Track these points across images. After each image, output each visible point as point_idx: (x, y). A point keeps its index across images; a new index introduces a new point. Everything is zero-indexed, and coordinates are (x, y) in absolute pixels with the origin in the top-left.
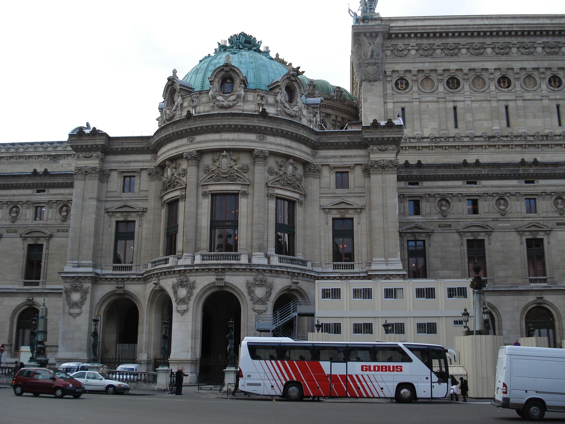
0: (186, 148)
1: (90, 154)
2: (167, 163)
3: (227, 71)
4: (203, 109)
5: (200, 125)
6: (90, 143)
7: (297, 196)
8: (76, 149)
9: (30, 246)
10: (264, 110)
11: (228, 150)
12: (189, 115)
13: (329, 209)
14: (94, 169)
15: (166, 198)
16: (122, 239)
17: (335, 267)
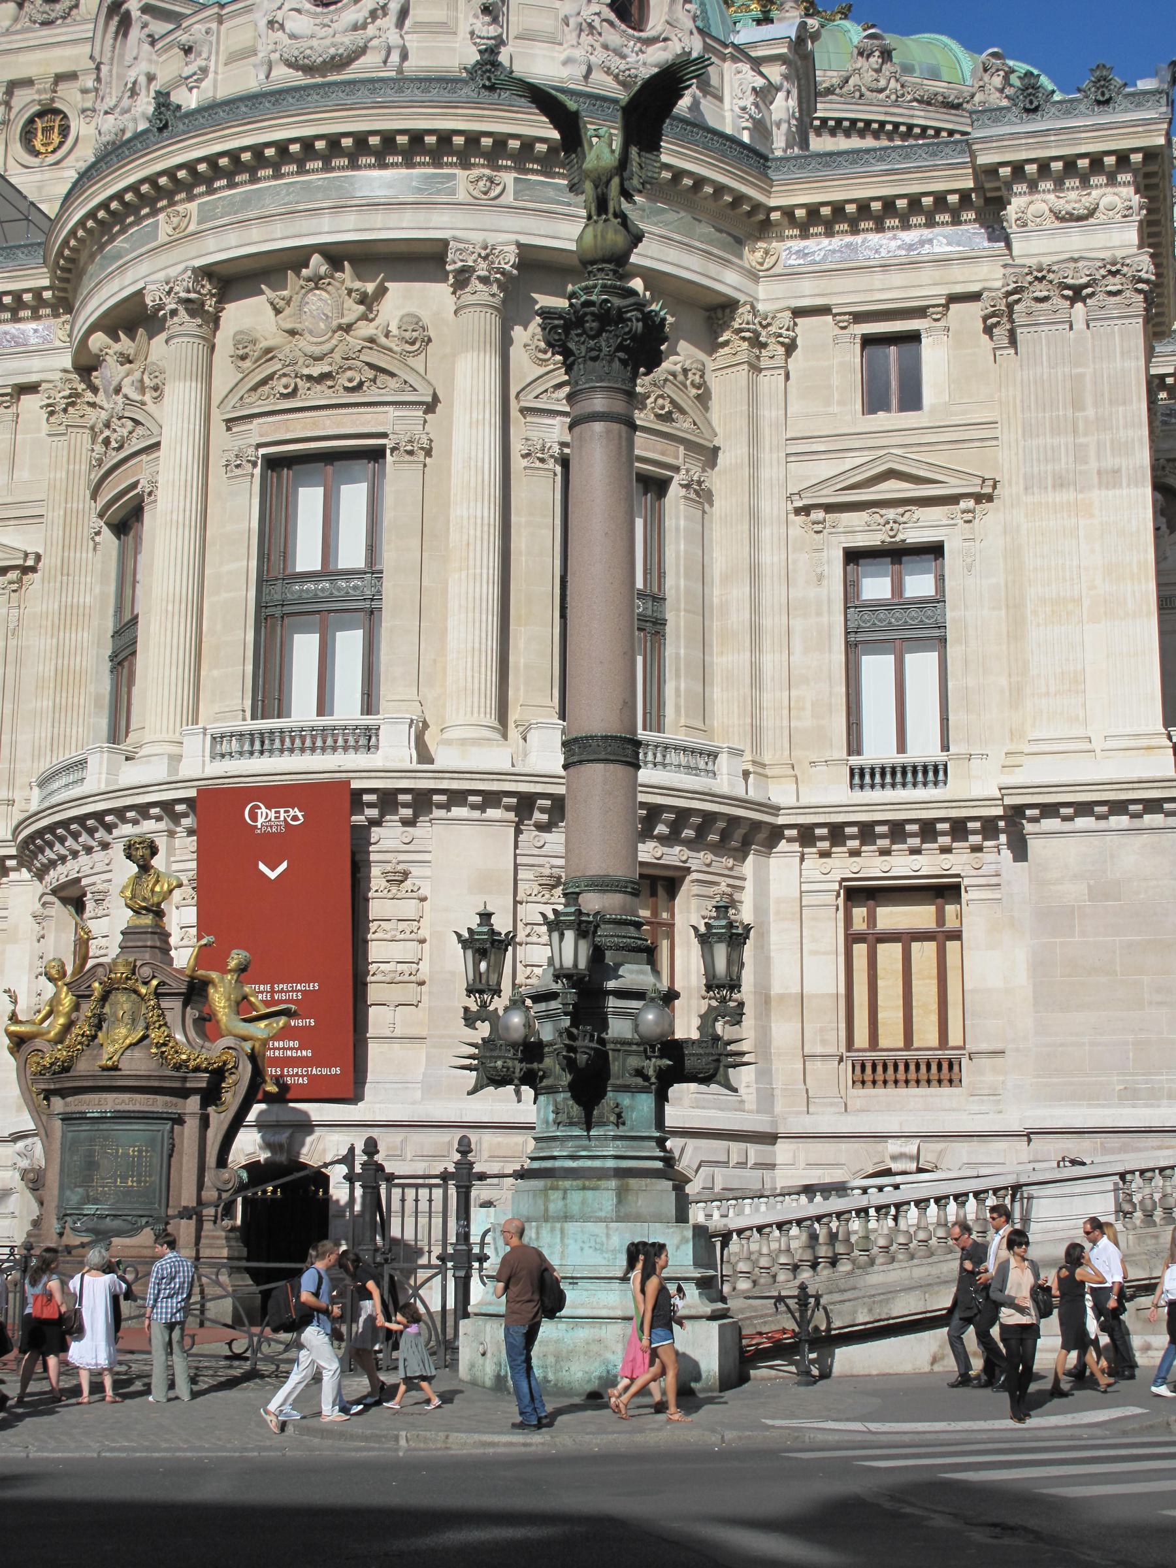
11: (336, 256)
12: (167, 119)
13: (830, 508)
17: (860, 777)
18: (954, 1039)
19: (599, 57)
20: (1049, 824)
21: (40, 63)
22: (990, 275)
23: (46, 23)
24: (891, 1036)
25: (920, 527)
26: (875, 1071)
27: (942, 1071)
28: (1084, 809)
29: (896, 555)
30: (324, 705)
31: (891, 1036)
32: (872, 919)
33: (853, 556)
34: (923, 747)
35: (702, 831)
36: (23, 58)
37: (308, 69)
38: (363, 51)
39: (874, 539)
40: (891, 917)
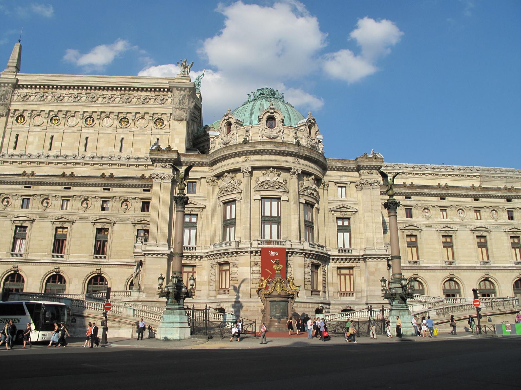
0: (243, 164)
1: (165, 165)
2: (226, 174)
3: (271, 113)
4: (253, 138)
5: (258, 149)
6: (165, 156)
7: (315, 202)
8: (154, 161)
9: (97, 229)
10: (298, 142)
11: (274, 168)
12: (245, 142)
13: (334, 211)
14: (168, 175)
15: (222, 199)
16: (187, 227)
17: (340, 251)
18: (352, 290)
19: (309, 142)
20: (370, 260)
21: (160, 110)
22: (358, 180)
23: (161, 104)
24: (343, 289)
25: (347, 215)
26: (341, 294)
27: (350, 294)
28: (375, 258)
29: (343, 219)
30: (271, 237)
31: (343, 289)
32: (340, 272)
33: (337, 218)
34: (347, 247)
35: (316, 257)
36: (156, 109)
37: (269, 138)
38: (278, 137)
39: (341, 216)
40: (343, 271)
